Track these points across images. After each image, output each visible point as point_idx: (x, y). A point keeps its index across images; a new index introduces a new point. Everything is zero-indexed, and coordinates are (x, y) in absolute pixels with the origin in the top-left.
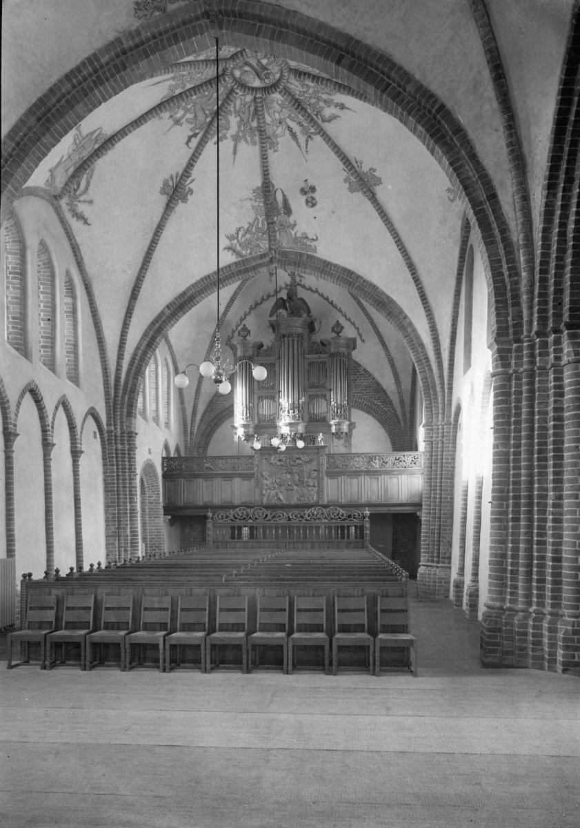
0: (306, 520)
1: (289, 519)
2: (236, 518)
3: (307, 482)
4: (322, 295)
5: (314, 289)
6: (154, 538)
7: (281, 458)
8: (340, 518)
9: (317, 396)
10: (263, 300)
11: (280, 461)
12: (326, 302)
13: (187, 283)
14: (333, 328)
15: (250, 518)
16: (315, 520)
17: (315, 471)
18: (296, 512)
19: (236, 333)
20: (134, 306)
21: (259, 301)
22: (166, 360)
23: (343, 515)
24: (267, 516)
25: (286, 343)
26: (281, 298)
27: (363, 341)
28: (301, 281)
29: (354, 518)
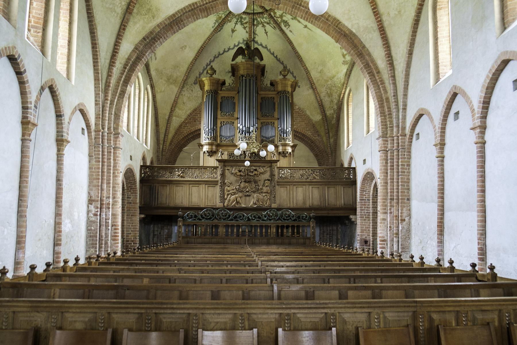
1: (249, 220)
3: (262, 189)
4: (269, 51)
5: (264, 45)
7: (241, 169)
9: (267, 124)
10: (224, 51)
11: (240, 171)
12: (272, 56)
13: (176, 6)
14: (281, 72)
15: (215, 218)
16: (270, 220)
17: (269, 180)
18: (255, 213)
19: (205, 72)
20: (128, 20)
21: (221, 52)
22: (147, 89)
23: (293, 217)
24: (229, 216)
25: (244, 81)
26: (241, 48)
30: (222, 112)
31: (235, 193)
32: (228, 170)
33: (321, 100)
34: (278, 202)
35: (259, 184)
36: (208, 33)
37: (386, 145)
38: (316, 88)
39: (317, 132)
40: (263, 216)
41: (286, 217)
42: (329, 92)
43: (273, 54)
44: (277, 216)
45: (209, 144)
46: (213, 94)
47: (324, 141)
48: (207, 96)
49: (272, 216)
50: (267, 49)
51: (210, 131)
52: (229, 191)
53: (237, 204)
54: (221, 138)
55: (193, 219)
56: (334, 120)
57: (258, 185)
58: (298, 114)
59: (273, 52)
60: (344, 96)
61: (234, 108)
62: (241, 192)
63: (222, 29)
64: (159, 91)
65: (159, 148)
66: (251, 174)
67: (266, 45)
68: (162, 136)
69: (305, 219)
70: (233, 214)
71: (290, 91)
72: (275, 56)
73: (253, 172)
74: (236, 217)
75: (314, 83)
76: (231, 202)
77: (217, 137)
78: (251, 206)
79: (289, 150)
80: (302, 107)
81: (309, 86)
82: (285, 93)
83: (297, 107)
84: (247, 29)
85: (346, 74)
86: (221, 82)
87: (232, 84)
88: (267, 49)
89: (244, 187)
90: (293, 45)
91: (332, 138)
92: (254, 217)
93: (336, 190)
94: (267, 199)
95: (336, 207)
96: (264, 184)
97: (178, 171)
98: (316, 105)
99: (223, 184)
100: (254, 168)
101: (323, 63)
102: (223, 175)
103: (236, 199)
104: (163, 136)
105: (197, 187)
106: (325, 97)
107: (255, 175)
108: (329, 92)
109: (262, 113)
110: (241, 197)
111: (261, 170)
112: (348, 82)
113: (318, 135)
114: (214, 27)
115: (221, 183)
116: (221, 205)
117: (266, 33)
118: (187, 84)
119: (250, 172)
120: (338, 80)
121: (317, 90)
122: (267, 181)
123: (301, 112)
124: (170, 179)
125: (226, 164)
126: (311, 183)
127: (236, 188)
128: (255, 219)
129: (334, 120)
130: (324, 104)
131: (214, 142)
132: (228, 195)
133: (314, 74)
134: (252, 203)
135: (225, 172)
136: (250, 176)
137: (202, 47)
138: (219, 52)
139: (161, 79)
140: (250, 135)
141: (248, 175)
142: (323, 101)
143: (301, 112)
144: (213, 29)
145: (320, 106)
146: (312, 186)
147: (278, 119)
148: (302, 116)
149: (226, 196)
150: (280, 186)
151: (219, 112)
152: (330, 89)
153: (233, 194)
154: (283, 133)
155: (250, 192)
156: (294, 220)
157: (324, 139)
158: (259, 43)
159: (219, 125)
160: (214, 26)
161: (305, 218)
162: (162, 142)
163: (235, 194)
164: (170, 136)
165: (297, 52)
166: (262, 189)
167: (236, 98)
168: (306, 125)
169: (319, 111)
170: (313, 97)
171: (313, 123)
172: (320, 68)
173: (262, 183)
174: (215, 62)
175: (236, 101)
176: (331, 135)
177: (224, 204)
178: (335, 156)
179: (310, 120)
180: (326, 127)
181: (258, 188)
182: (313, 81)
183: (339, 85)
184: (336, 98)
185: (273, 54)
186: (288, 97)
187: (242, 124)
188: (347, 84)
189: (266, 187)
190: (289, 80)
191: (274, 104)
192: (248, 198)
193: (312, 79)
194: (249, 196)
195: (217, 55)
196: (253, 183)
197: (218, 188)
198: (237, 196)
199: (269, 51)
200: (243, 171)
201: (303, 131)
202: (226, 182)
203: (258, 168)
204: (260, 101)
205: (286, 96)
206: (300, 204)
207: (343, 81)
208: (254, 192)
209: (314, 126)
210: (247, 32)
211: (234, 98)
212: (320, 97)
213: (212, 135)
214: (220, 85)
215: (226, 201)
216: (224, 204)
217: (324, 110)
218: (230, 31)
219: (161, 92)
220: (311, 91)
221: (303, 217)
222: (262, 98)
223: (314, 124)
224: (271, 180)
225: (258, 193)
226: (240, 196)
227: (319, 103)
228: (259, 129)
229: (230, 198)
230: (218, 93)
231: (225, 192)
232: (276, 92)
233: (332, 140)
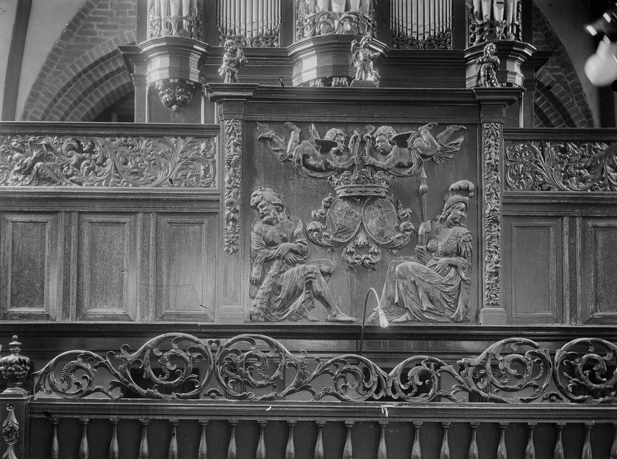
2: (147, 383)
52: (271, 244)
66: (381, 162)
73: (385, 153)
76: (282, 295)
119: (374, 150)
122: (458, 197)
136: (375, 168)
153: (291, 256)
200: (341, 146)
202: (254, 200)
226: (325, 268)
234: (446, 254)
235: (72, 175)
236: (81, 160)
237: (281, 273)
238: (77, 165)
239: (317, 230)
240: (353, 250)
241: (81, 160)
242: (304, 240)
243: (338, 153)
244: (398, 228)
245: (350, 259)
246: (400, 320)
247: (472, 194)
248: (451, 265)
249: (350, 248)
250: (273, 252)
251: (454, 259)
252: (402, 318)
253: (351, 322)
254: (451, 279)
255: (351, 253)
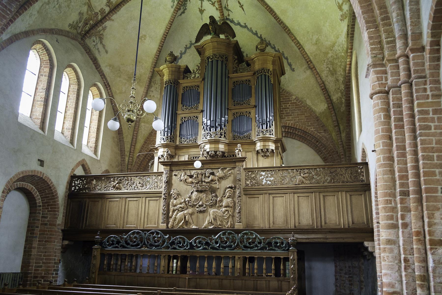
0: (213, 248)
1: (192, 247)
4: (251, 30)
5: (242, 24)
6: (41, 267)
7: (192, 174)
8: (256, 246)
11: (191, 176)
12: (256, 36)
15: (144, 244)
16: (225, 248)
17: (231, 188)
23: (260, 243)
24: (164, 242)
25: (210, 63)
27: (293, 70)
28: (229, 15)
29: (276, 246)
30: (183, 106)
31: (183, 208)
32: (175, 175)
33: (323, 83)
34: (244, 219)
35: (218, 194)
36: (168, 15)
37: (384, 82)
38: (314, 67)
39: (323, 127)
40: (213, 241)
41: (250, 243)
42: (331, 69)
43: (256, 34)
44: (233, 241)
45: (164, 146)
46: (173, 85)
47: (334, 137)
48: (165, 88)
49: (226, 242)
50: (248, 29)
51: (166, 130)
53: (186, 225)
54: (181, 138)
55: (114, 246)
56: (343, 106)
57: (216, 196)
58: (296, 105)
59: (256, 31)
60: (350, 67)
61: (199, 99)
62: (194, 206)
63: (186, 9)
64: (118, 92)
65: (124, 161)
67: (245, 24)
68: (127, 147)
69: (279, 247)
70: (169, 238)
71: (271, 69)
72: (259, 36)
73: (209, 177)
74: (173, 243)
75: (310, 61)
76: (177, 221)
77: (176, 137)
78: (205, 227)
79: (272, 146)
80: (300, 96)
81: (306, 66)
82: (263, 71)
83: (294, 97)
84: (216, 4)
85: (348, 35)
86: (182, 70)
87: (197, 70)
88: (248, 29)
89: (197, 200)
90: (275, 14)
91: (343, 132)
92: (200, 242)
93: (338, 199)
94: (228, 216)
95: (339, 227)
96: (224, 194)
97: (114, 181)
98: (318, 90)
99: (168, 196)
100: (210, 171)
101: (318, 30)
102: (169, 183)
103: (185, 217)
104: (129, 146)
105: (135, 202)
106: (327, 76)
107: (212, 180)
108: (331, 69)
109: (234, 101)
110: (191, 214)
111: (219, 173)
112: (352, 45)
113: (325, 131)
114: (174, 7)
115: (164, 194)
116: (163, 226)
117: (241, 6)
118: (155, 83)
120: (339, 48)
121: (316, 69)
122: (229, 189)
123: (299, 102)
124: (103, 192)
125: (173, 168)
126: (295, 190)
127: (185, 202)
128: (200, 247)
129: (343, 106)
130: (327, 87)
131: (172, 143)
132: (174, 211)
133: (309, 48)
134: (206, 222)
135: (172, 179)
137: (164, 34)
138: (191, 42)
139: (120, 77)
140: (216, 130)
141: (202, 181)
142: (326, 83)
143: (299, 102)
144: (172, 10)
145: (322, 90)
146: (299, 195)
147: (255, 106)
148: (300, 107)
149: (171, 213)
150: (248, 196)
151: (180, 106)
152: (332, 64)
153: (180, 209)
154: (262, 125)
155: (205, 206)
156: (262, 249)
157: (334, 134)
158: (236, 22)
159: (179, 122)
160: (173, 5)
161: (280, 245)
162: (127, 154)
163: (182, 209)
164: (139, 146)
165: (282, 22)
166: (221, 201)
167: (202, 86)
168: (307, 119)
169: (322, 98)
170: (312, 81)
171: (316, 115)
172: (315, 38)
173: (222, 193)
174: (187, 54)
175: (201, 90)
176: (341, 127)
177: (167, 225)
178: (349, 157)
179: (311, 111)
180: (334, 118)
181: (216, 201)
182: (309, 58)
183: (343, 54)
184: (341, 74)
185: (256, 34)
186: (269, 77)
187: (207, 118)
188: (352, 49)
189: (228, 198)
190: (268, 54)
191: (251, 87)
192: (201, 215)
193: (308, 56)
194: (204, 212)
195: (188, 46)
196: (210, 193)
197: (162, 202)
198: (185, 212)
199: (251, 30)
201: (302, 127)
203: (215, 171)
204: (231, 86)
205: (265, 75)
206: (280, 223)
207: (346, 46)
208: (211, 206)
209: (317, 119)
210: (217, 9)
211: (198, 86)
212: (321, 79)
213: (169, 135)
214: (182, 74)
215: (171, 220)
216: (167, 225)
217: (329, 95)
218: (198, 12)
219: (121, 93)
220: (309, 72)
221: (276, 243)
222: (234, 82)
223: (318, 117)
224: (235, 187)
225: (215, 208)
227: (321, 87)
228: (230, 123)
229: (176, 215)
230: (179, 82)
231: (171, 207)
232: (251, 73)
233: (343, 135)
234: (226, 207)
235: (126, 187)
236: (128, 183)
237: (177, 214)
238: (127, 184)
239: (188, 201)
240: (198, 206)
241: (128, 183)
242: (184, 204)
243: (195, 178)
244: (211, 200)
245: (197, 209)
246: (211, 228)
247: (233, 188)
248: (226, 210)
249: (197, 206)
250: (175, 208)
251: (227, 209)
252: (212, 227)
253: (196, 228)
254: (226, 215)
255: (197, 208)
